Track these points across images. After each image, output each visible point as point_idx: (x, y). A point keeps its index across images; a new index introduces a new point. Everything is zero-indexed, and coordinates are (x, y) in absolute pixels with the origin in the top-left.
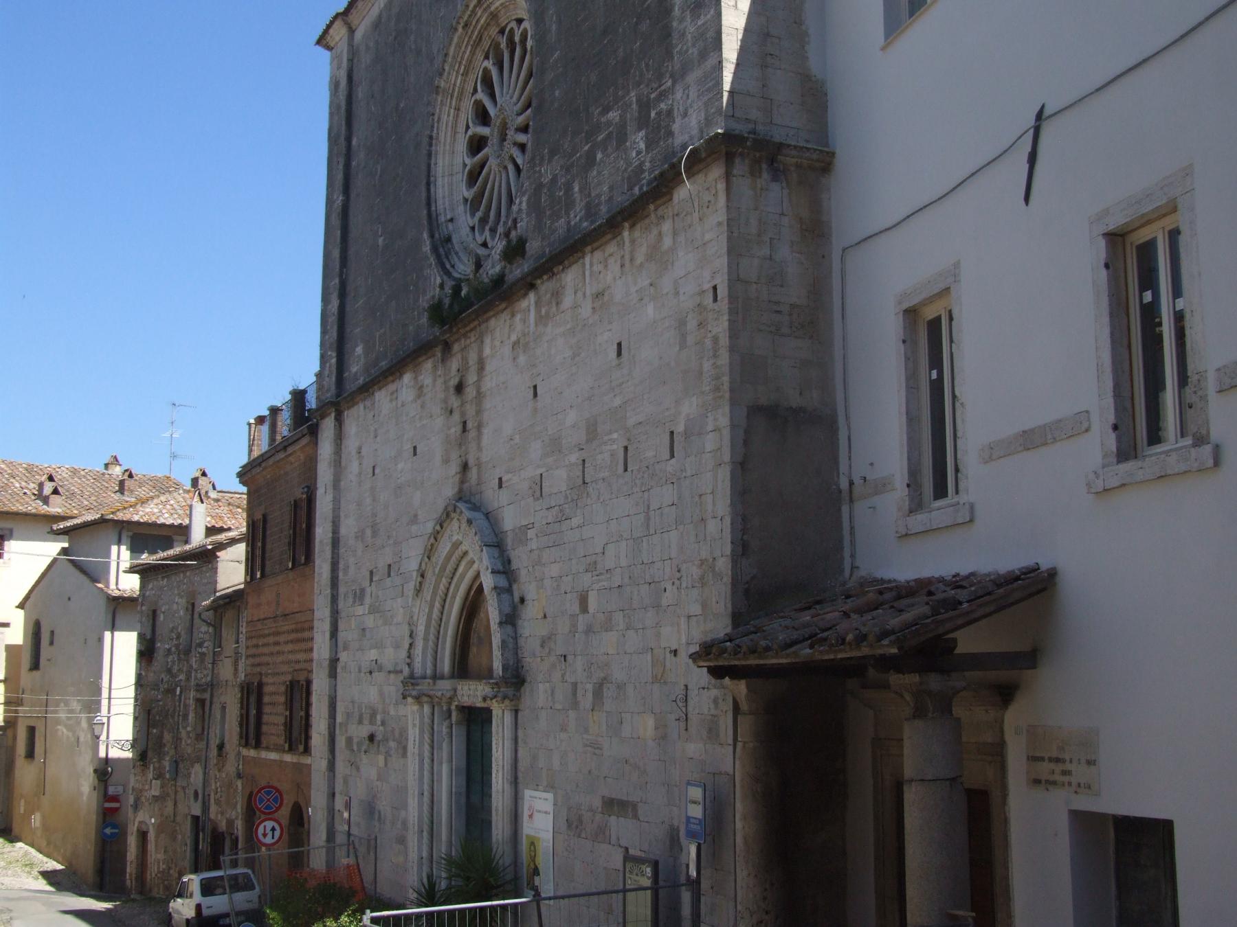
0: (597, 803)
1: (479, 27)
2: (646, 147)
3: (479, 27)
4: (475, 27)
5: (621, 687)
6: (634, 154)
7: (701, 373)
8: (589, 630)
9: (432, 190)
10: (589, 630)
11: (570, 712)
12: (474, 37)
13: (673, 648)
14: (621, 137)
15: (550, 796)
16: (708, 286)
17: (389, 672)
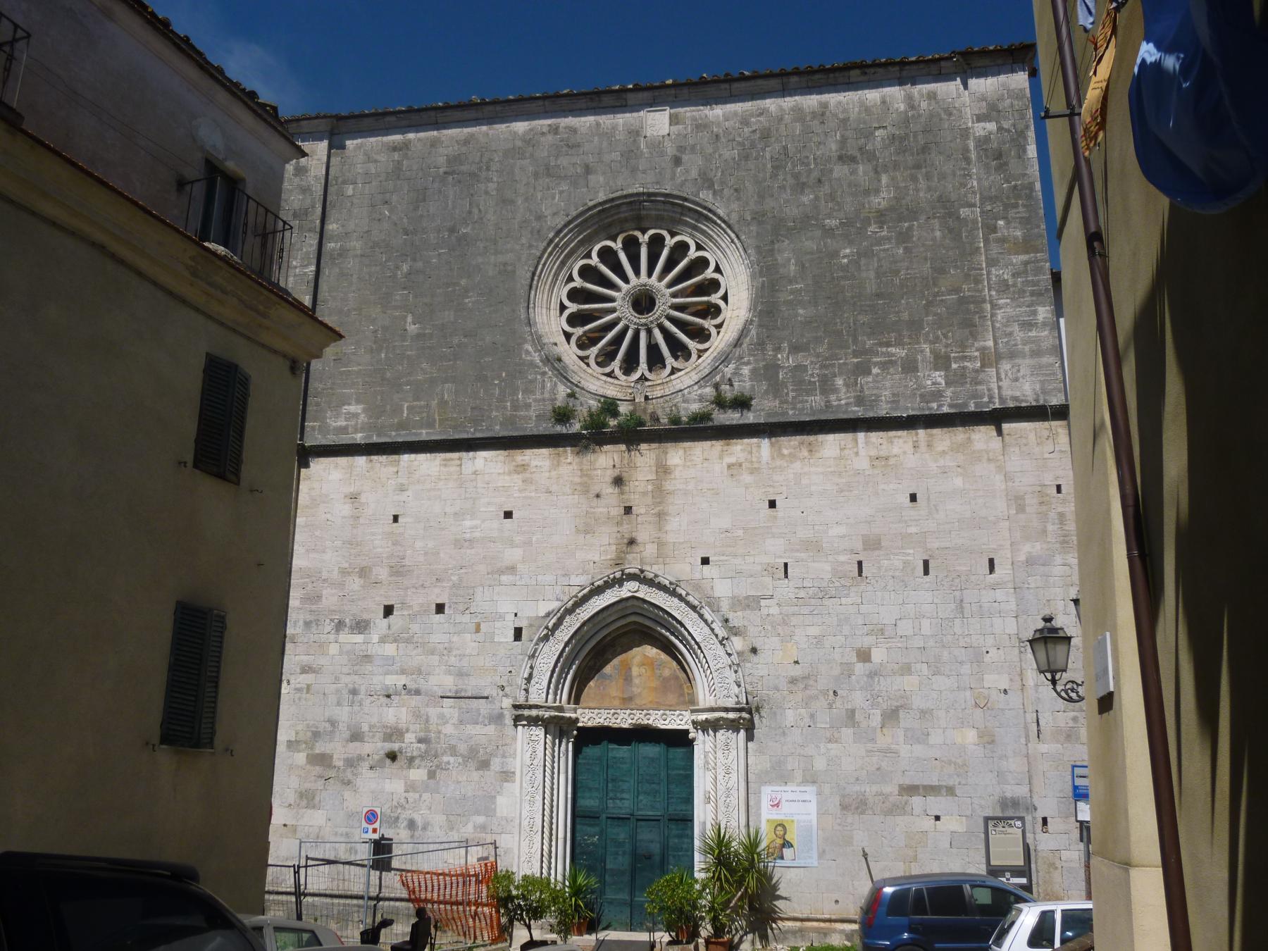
0: (891, 789)
1: (616, 217)
2: (946, 384)
3: (616, 217)
4: (612, 216)
5: (924, 713)
6: (929, 382)
7: (1044, 531)
8: (872, 675)
9: (532, 315)
10: (872, 675)
11: (844, 729)
12: (606, 221)
13: (1003, 688)
14: (910, 367)
15: (811, 790)
16: (1050, 480)
17: (442, 697)
